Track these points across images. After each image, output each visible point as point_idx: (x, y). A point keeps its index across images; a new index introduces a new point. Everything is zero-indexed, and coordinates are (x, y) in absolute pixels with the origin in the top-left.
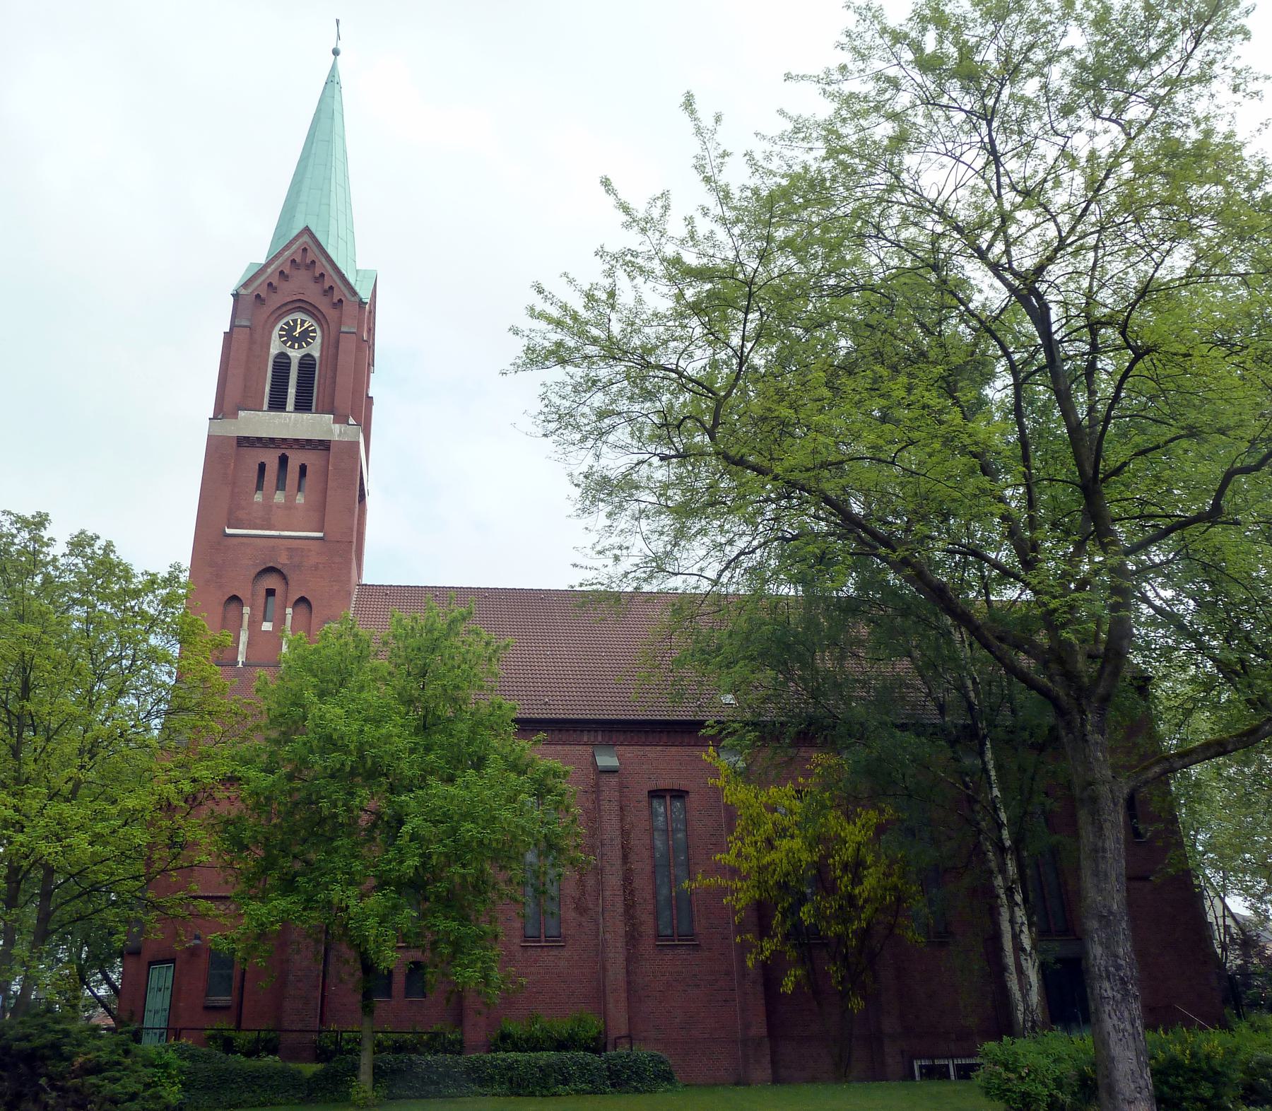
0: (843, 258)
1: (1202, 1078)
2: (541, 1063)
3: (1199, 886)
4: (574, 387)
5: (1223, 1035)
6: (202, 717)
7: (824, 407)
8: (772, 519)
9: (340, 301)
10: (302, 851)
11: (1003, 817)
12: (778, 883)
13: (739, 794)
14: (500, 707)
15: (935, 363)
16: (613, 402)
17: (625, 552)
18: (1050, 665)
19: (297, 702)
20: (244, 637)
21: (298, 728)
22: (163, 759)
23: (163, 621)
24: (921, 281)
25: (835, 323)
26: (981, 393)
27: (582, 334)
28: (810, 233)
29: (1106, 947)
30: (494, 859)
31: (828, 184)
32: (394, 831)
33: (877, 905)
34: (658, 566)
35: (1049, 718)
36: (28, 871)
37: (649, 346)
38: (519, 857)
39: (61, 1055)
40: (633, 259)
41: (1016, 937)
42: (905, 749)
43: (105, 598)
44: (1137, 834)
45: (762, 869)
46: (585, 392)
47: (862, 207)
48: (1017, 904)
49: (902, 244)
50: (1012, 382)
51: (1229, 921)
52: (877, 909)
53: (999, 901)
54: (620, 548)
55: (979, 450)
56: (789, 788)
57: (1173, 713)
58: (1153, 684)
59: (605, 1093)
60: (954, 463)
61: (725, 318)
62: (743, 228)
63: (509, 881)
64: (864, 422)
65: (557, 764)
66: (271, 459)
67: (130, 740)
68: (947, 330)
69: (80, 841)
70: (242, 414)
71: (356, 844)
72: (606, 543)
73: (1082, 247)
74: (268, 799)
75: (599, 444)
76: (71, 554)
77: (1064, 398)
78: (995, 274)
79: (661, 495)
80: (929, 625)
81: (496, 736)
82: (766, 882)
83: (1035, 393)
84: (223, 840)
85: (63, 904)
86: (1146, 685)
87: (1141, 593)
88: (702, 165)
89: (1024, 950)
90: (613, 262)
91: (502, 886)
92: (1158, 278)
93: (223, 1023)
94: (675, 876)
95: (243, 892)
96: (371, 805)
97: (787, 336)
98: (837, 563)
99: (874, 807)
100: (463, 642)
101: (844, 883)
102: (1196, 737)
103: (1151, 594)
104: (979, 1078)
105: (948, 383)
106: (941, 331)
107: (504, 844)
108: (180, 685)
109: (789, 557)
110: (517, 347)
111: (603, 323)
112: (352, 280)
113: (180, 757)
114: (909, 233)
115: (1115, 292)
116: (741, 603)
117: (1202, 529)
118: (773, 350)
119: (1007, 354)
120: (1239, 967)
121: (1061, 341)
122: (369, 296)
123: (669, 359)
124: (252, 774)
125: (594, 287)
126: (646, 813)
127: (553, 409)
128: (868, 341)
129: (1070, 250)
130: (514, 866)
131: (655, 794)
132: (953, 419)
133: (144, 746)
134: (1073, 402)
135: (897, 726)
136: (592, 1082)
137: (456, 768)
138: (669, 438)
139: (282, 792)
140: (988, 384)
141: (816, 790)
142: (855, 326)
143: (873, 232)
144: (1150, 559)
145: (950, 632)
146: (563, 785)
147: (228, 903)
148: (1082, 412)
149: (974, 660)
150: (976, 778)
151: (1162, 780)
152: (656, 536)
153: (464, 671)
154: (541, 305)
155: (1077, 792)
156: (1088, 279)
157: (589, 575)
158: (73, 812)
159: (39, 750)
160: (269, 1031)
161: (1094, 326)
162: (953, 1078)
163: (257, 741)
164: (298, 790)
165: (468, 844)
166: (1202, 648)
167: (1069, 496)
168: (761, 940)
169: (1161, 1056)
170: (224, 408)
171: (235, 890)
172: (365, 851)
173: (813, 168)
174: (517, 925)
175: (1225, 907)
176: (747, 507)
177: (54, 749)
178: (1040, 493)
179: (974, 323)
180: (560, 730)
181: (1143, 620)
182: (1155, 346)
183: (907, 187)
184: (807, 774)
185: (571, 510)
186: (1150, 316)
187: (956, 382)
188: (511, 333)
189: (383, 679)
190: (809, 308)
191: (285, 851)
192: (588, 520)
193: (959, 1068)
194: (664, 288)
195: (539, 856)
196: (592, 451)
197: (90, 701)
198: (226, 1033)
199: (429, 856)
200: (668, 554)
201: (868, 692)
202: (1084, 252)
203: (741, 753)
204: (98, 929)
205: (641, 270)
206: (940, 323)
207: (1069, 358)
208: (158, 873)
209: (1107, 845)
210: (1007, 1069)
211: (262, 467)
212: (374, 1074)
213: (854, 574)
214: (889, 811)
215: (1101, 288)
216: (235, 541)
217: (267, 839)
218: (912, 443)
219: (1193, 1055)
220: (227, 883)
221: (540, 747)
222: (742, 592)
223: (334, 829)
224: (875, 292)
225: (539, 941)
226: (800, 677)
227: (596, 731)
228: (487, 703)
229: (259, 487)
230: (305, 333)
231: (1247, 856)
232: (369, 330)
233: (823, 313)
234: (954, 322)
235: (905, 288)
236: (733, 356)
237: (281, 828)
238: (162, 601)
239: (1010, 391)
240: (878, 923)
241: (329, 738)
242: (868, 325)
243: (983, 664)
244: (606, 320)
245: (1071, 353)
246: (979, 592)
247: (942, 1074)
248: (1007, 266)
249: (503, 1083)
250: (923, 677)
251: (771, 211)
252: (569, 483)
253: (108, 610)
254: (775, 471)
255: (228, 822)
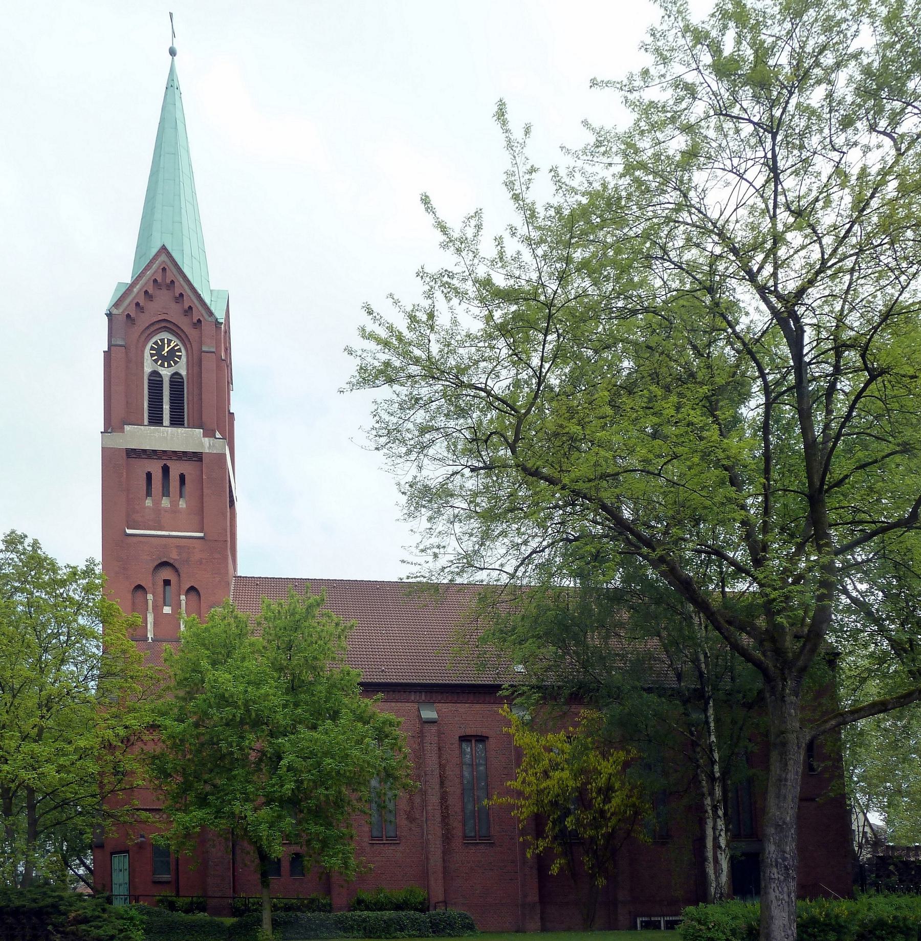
0: (632, 280)
1: (831, 930)
2: (385, 918)
3: (850, 805)
4: (400, 405)
5: (849, 903)
6: (126, 680)
7: (606, 424)
8: (559, 523)
9: (199, 321)
10: (210, 778)
11: (716, 756)
12: (551, 802)
13: (525, 739)
14: (348, 674)
15: (702, 384)
16: (433, 418)
17: (442, 550)
18: (765, 643)
19: (196, 669)
20: (150, 618)
21: (198, 689)
22: (101, 712)
23: (87, 605)
24: (697, 303)
25: (620, 345)
26: (737, 412)
27: (406, 354)
28: (605, 254)
29: (778, 845)
30: (348, 784)
31: (623, 203)
32: (275, 764)
33: (620, 817)
34: (468, 563)
35: (759, 684)
36: (16, 791)
37: (463, 366)
38: (366, 783)
39: (59, 911)
40: (449, 280)
41: (716, 839)
42: (649, 707)
43: (40, 587)
44: (811, 768)
45: (540, 792)
46: (409, 409)
47: (651, 228)
48: (719, 817)
49: (684, 266)
50: (764, 401)
51: (867, 829)
52: (620, 820)
53: (707, 815)
54: (438, 547)
55: (730, 463)
56: (562, 735)
57: (852, 680)
58: (840, 659)
59: (428, 937)
60: (708, 475)
61: (528, 340)
62: (546, 248)
63: (360, 799)
64: (638, 438)
65: (392, 717)
66: (155, 468)
67: (75, 697)
68: (715, 352)
69: (50, 770)
70: (127, 428)
71: (248, 773)
72: (427, 543)
73: (840, 270)
74: (182, 741)
75: (421, 456)
76: (7, 550)
77: (805, 416)
78: (761, 297)
79: (471, 502)
80: (676, 612)
81: (346, 695)
82: (542, 801)
83: (782, 412)
84: (153, 770)
85: (44, 813)
86: (835, 659)
87: (842, 586)
88: (511, 182)
89: (720, 847)
90: (432, 284)
91: (355, 802)
92: (902, 301)
93: (167, 892)
94: (478, 796)
95: (171, 806)
96: (257, 745)
97: (579, 357)
98: (608, 561)
99: (623, 749)
100: (318, 623)
101: (598, 802)
102: (865, 699)
103: (850, 587)
104: (680, 929)
105: (710, 402)
106: (710, 352)
107: (355, 774)
108: (107, 656)
109: (571, 555)
110: (351, 366)
111: (424, 344)
112: (207, 300)
113: (113, 710)
114: (691, 254)
115: (862, 316)
116: (532, 592)
117: (899, 533)
118: (567, 370)
119: (763, 375)
120: (869, 859)
121: (810, 363)
122: (224, 316)
123: (478, 379)
124: (168, 722)
125: (416, 308)
126: (457, 752)
127: (383, 425)
128: (647, 362)
129: (829, 272)
130: (363, 789)
131: (464, 739)
132: (712, 436)
133: (86, 701)
134: (812, 421)
135: (645, 690)
136: (420, 930)
137: (318, 719)
138: (478, 451)
139: (191, 736)
140: (744, 403)
141: (581, 736)
142: (637, 347)
143: (660, 253)
144: (854, 558)
145: (691, 617)
146: (397, 732)
147: (161, 814)
148: (818, 430)
149: (707, 639)
150: (699, 728)
151: (836, 730)
152: (467, 537)
153: (320, 646)
154: (371, 327)
155: (772, 738)
156: (841, 302)
157: (414, 569)
158: (42, 750)
159: (8, 704)
160: (199, 897)
161: (839, 348)
162: (663, 928)
163: (169, 699)
164: (203, 734)
165: (329, 774)
166: (882, 630)
167: (797, 504)
168: (537, 840)
169: (805, 915)
170: (112, 424)
171: (165, 805)
172: (255, 778)
173: (611, 186)
174: (366, 829)
175: (866, 819)
176: (539, 513)
177: (20, 704)
178: (775, 502)
179: (738, 345)
180: (394, 691)
181: (841, 608)
182: (889, 367)
183: (692, 206)
184: (576, 725)
185: (399, 514)
186: (889, 340)
187: (717, 401)
188: (346, 353)
189: (259, 651)
190: (599, 330)
191: (198, 778)
192: (413, 524)
193: (667, 922)
194: (476, 309)
195: (380, 782)
196: (416, 463)
197: (41, 667)
198: (169, 899)
199: (302, 782)
200: (476, 552)
201: (625, 664)
202: (841, 275)
203: (528, 709)
204: (71, 831)
205: (457, 291)
206: (709, 346)
207: (815, 379)
208: (109, 793)
209: (789, 776)
210: (700, 922)
211: (149, 476)
212: (273, 924)
213: (621, 570)
214: (634, 752)
215: (850, 311)
216: (135, 539)
217: (184, 769)
218: (676, 457)
219: (827, 915)
220: (158, 799)
221: (380, 704)
222: (533, 584)
223: (232, 763)
224: (657, 314)
225: (382, 840)
226: (574, 652)
227: (420, 692)
228: (338, 670)
229: (149, 493)
230: (172, 352)
231: (888, 784)
232: (226, 349)
233: (611, 335)
234: (721, 344)
235: (683, 310)
236: (533, 376)
237: (193, 761)
238: (83, 589)
239: (761, 410)
240: (620, 829)
241: (222, 697)
242: (648, 347)
243: (714, 643)
244: (427, 341)
245: (817, 374)
246: (717, 585)
247: (656, 926)
248: (773, 289)
249: (360, 930)
250: (667, 652)
251: (571, 231)
252: (397, 491)
253: (43, 596)
254: (564, 482)
255: (154, 757)
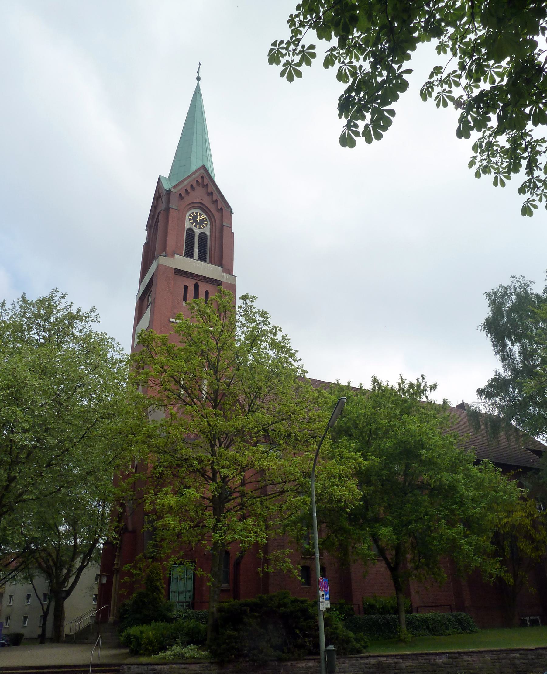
211: (186, 287)
230: (202, 221)
